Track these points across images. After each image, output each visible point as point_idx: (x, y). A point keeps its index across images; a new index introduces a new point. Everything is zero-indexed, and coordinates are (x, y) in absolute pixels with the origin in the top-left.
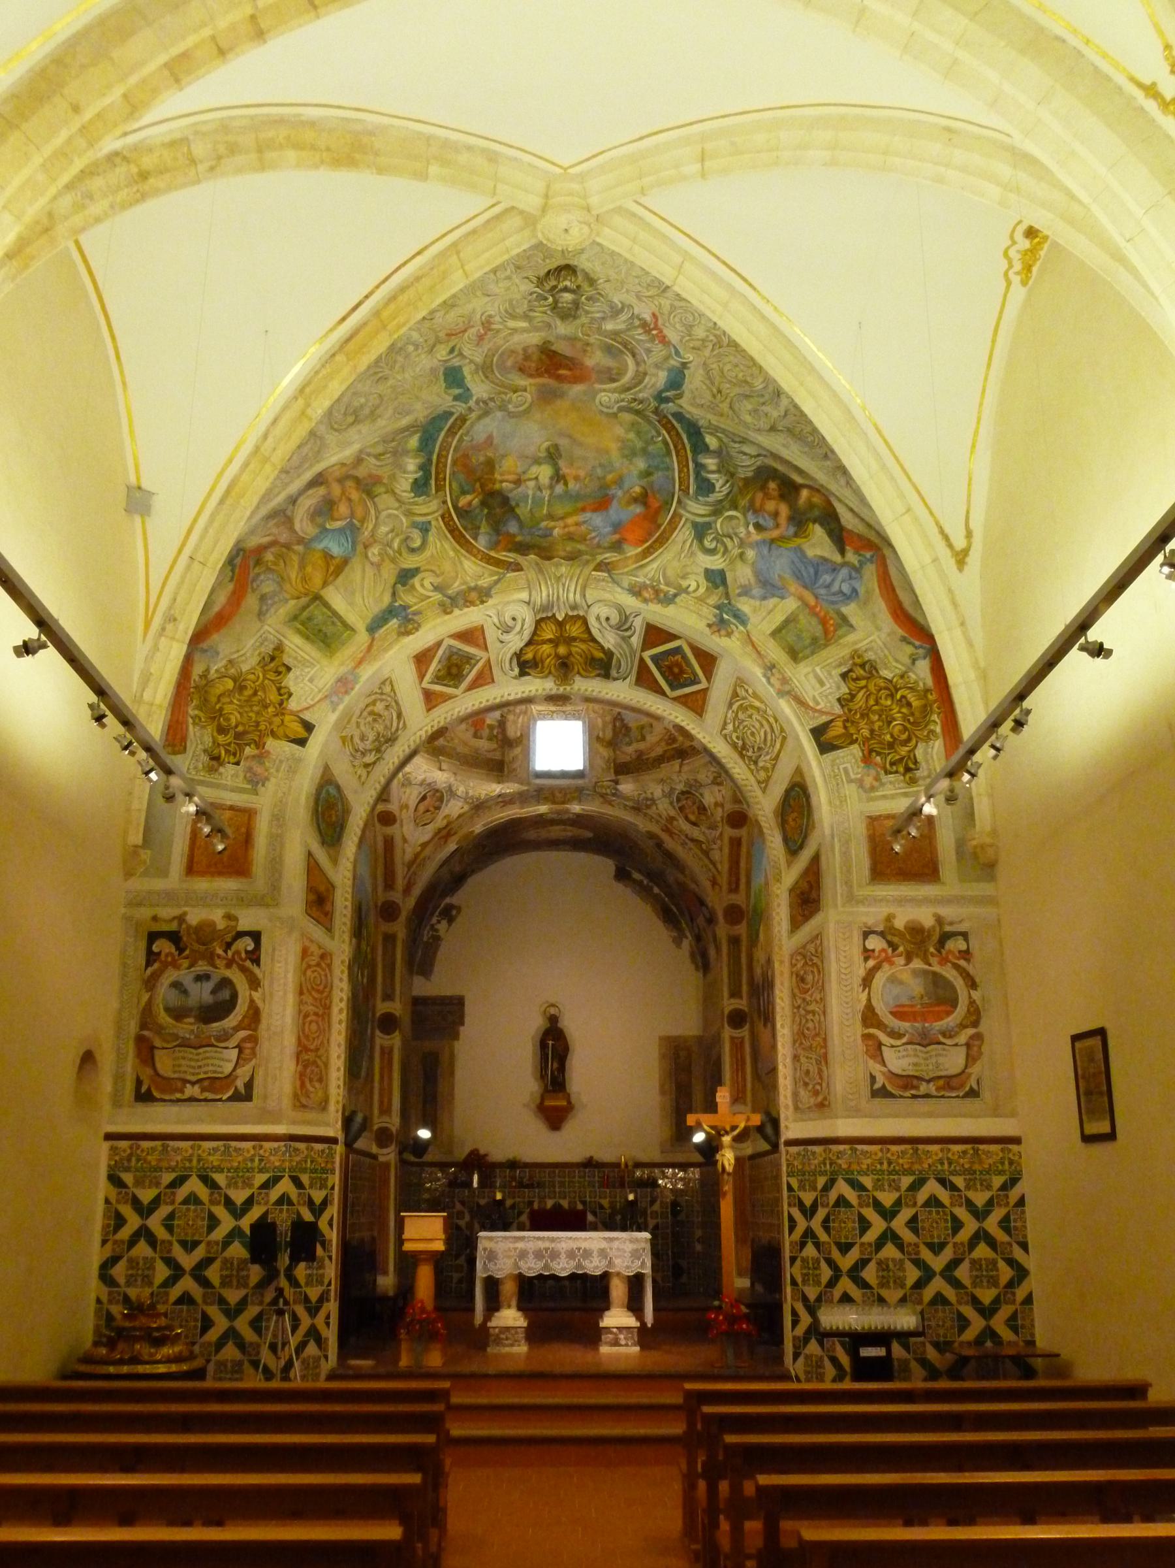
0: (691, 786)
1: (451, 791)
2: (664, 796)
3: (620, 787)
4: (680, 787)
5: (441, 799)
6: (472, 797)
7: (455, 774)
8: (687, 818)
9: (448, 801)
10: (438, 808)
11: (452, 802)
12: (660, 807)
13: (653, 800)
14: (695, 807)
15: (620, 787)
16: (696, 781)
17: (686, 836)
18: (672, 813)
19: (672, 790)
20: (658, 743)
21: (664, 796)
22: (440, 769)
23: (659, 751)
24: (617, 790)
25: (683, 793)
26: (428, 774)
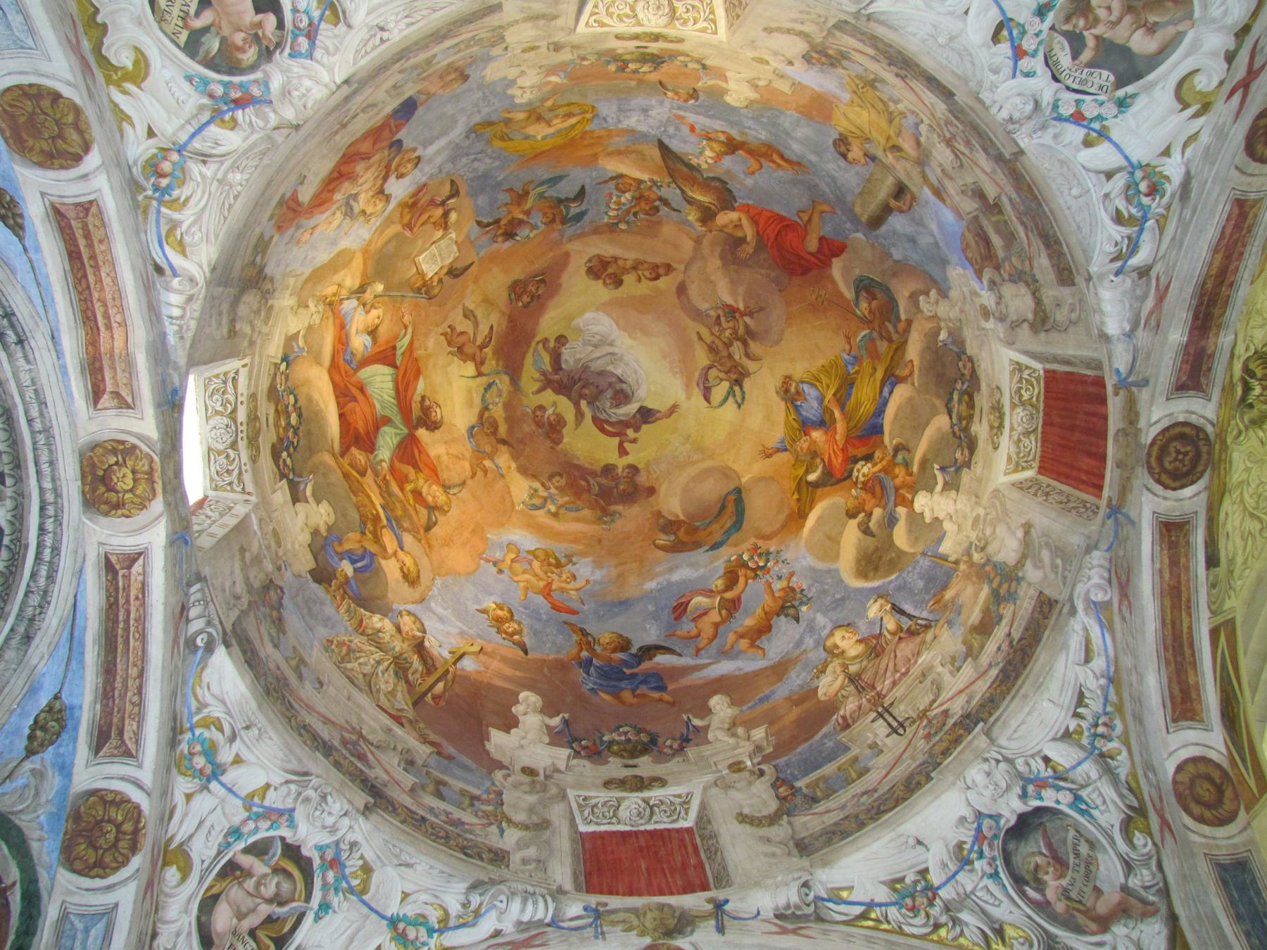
0: (335, 863)
1: (227, 107)
2: (248, 801)
3: (221, 653)
4: (309, 835)
5: (226, 62)
6: (181, 176)
7: (297, 127)
8: (209, 903)
9: (203, 86)
10: (192, 47)
11: (192, 100)
12: (203, 803)
13: (217, 771)
14: (265, 910)
15: (221, 653)
16: (367, 869)
17: (154, 935)
18: (203, 850)
19: (287, 815)
20: (327, 721)
21: (248, 801)
22: (346, 82)
23: (325, 732)
24: (209, 648)
25: (292, 851)
26: (354, 40)
